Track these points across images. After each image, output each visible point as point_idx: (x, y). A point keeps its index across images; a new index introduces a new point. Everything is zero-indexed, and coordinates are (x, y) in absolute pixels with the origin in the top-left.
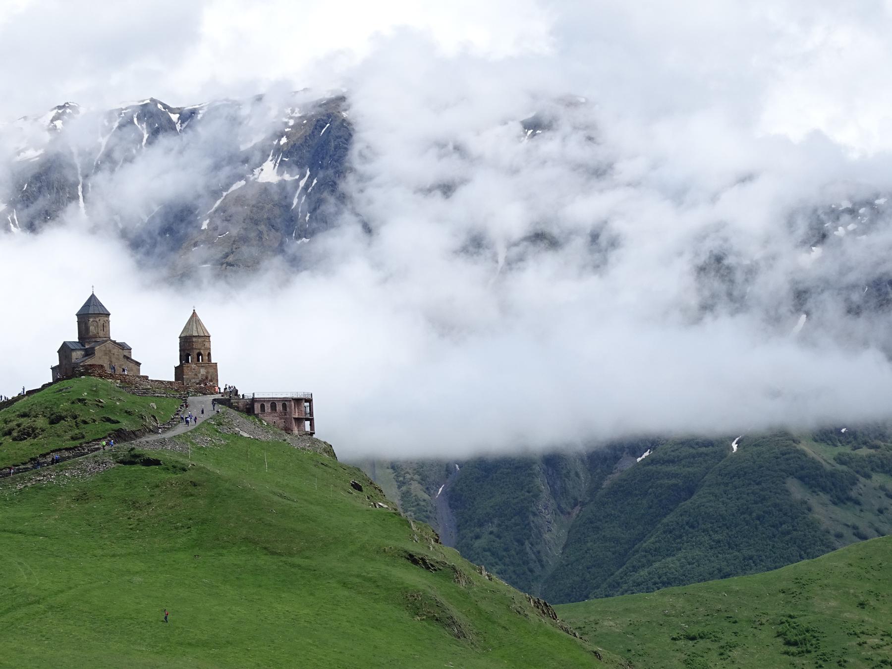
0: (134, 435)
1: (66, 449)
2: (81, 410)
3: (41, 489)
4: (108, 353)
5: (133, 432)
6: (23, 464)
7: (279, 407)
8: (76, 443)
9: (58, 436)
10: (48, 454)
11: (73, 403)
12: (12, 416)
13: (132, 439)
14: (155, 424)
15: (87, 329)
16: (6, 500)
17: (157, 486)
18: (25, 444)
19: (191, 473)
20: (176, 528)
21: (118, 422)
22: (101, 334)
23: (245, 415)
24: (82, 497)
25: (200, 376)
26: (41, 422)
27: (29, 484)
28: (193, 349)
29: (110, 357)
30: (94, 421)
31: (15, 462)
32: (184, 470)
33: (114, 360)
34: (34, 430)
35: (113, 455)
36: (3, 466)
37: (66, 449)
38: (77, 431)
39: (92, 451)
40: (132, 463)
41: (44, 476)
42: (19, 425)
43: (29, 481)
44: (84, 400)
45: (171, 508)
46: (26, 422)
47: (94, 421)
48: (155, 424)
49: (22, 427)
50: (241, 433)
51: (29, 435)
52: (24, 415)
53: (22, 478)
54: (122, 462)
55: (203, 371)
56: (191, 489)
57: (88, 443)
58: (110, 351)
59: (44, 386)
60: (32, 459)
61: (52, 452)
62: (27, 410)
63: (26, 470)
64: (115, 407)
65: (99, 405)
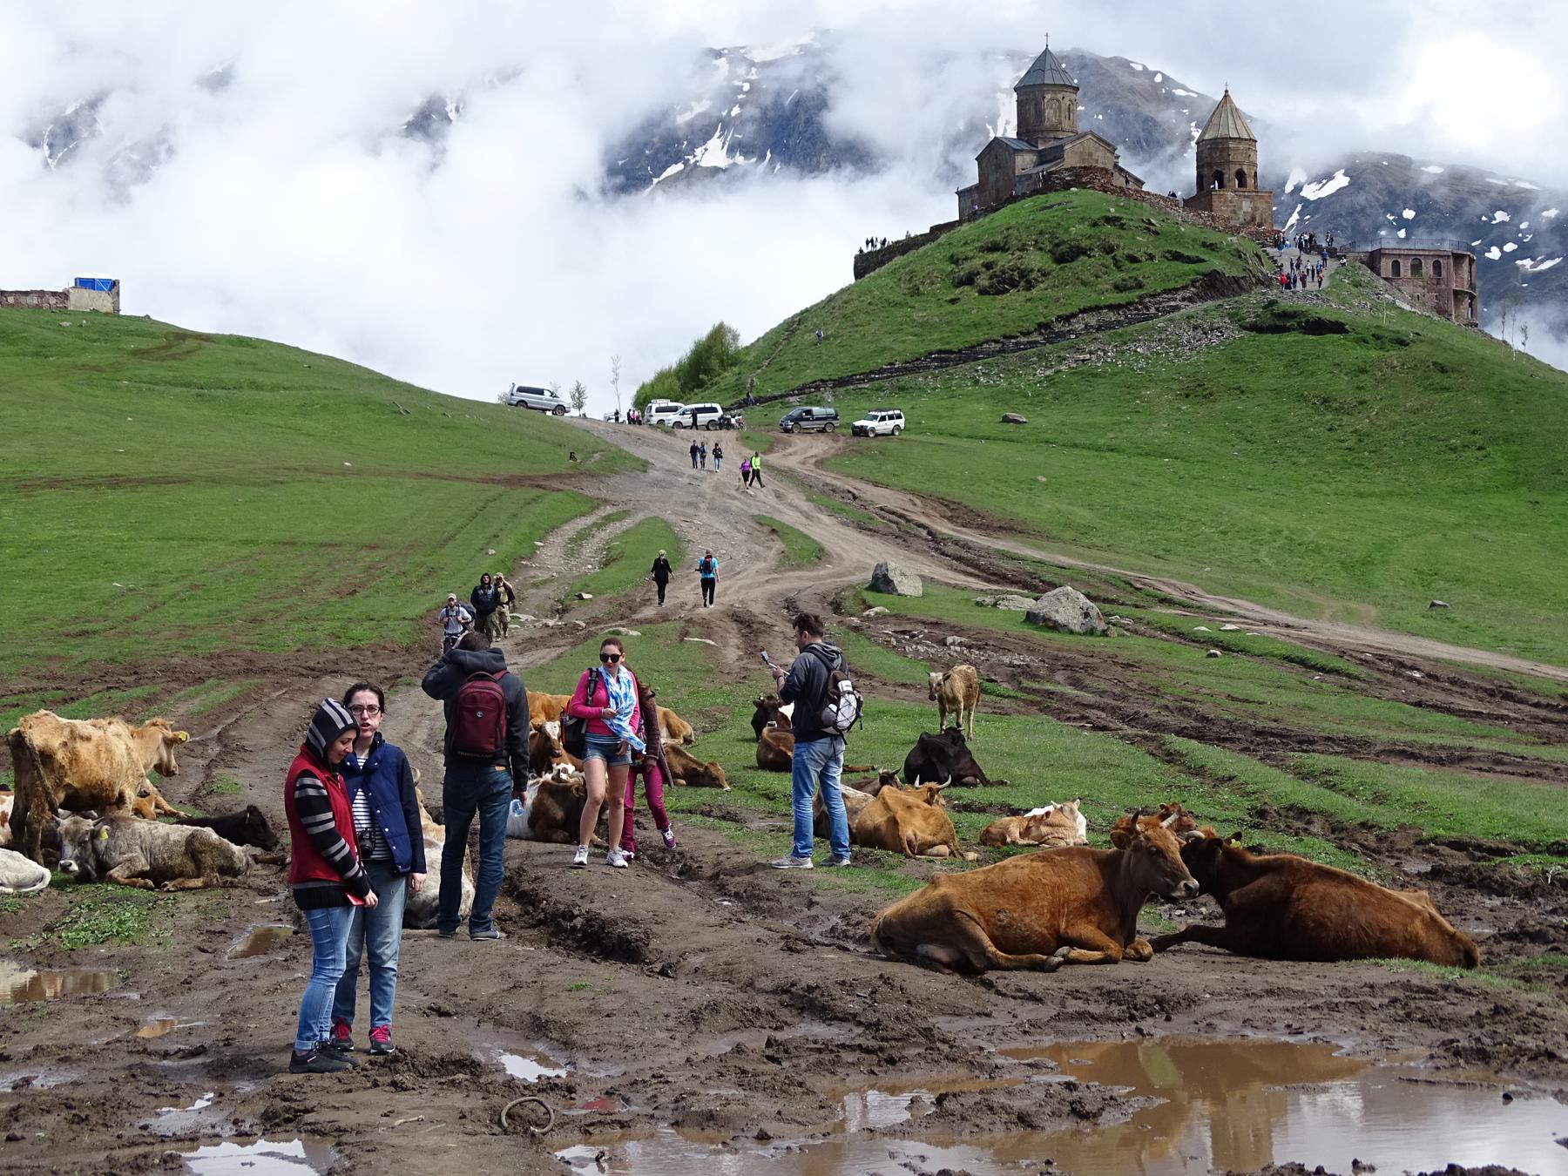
1: (1111, 307)
2: (1120, 237)
3: (1095, 375)
5: (1236, 280)
6: (1024, 334)
7: (1428, 268)
8: (1132, 296)
9: (1084, 283)
10: (1074, 315)
11: (1095, 224)
12: (969, 251)
13: (1236, 294)
15: (1040, 114)
16: (1026, 396)
17: (1363, 371)
18: (1015, 298)
20: (1453, 449)
22: (1066, 124)
24: (1197, 391)
25: (1241, 214)
26: (1036, 260)
27: (1063, 368)
28: (1229, 162)
30: (1151, 257)
31: (1007, 331)
32: (1402, 343)
34: (1024, 274)
35: (1230, 316)
36: (982, 338)
37: (1111, 307)
38: (1122, 275)
39: (1166, 312)
41: (1091, 353)
42: (988, 266)
43: (1060, 363)
44: (1118, 219)
45: (1416, 411)
46: (1003, 260)
49: (997, 269)
51: (1014, 284)
52: (994, 248)
53: (1042, 357)
54: (1256, 328)
55: (1246, 206)
56: (1438, 378)
57: (1154, 296)
59: (937, 230)
60: (1040, 325)
61: (1083, 311)
62: (999, 238)
63: (1034, 344)
64: (1182, 235)
65: (1148, 228)
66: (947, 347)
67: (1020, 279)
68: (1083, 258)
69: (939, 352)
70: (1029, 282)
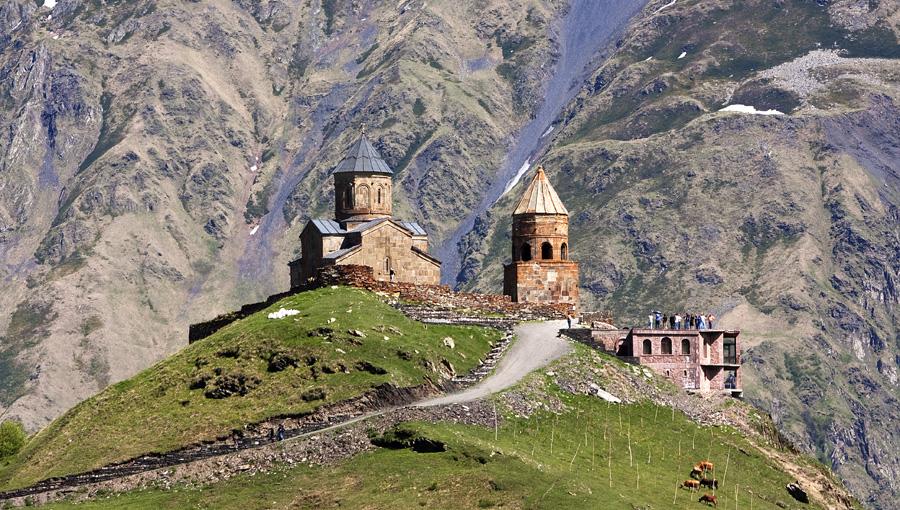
0: (408, 394)
4: (384, 242)
5: (408, 391)
12: (208, 354)
14: (447, 376)
19: (492, 466)
21: (383, 372)
23: (613, 361)
25: (546, 284)
29: (388, 250)
33: (394, 255)
40: (395, 446)
46: (232, 368)
47: (343, 369)
48: (447, 376)
50: (601, 393)
55: (552, 276)
58: (388, 239)
60: (235, 432)
65: (352, 339)
66: (158, 450)
67: (237, 387)
68: (291, 367)
69: (152, 454)
70: (244, 389)
